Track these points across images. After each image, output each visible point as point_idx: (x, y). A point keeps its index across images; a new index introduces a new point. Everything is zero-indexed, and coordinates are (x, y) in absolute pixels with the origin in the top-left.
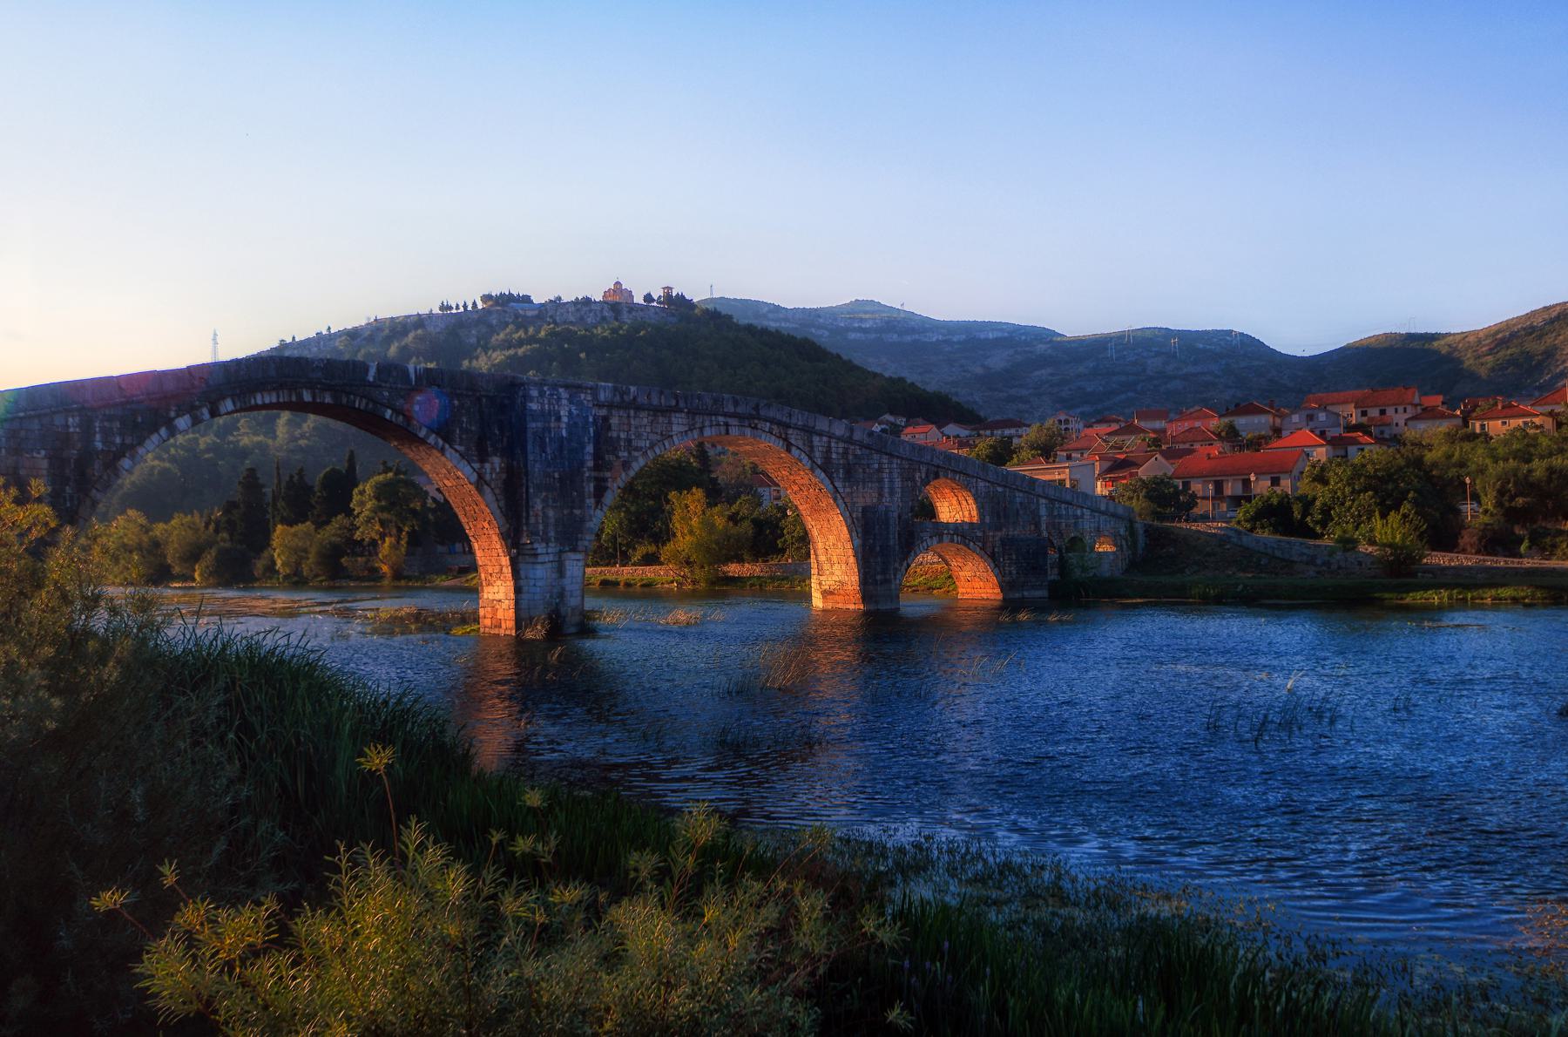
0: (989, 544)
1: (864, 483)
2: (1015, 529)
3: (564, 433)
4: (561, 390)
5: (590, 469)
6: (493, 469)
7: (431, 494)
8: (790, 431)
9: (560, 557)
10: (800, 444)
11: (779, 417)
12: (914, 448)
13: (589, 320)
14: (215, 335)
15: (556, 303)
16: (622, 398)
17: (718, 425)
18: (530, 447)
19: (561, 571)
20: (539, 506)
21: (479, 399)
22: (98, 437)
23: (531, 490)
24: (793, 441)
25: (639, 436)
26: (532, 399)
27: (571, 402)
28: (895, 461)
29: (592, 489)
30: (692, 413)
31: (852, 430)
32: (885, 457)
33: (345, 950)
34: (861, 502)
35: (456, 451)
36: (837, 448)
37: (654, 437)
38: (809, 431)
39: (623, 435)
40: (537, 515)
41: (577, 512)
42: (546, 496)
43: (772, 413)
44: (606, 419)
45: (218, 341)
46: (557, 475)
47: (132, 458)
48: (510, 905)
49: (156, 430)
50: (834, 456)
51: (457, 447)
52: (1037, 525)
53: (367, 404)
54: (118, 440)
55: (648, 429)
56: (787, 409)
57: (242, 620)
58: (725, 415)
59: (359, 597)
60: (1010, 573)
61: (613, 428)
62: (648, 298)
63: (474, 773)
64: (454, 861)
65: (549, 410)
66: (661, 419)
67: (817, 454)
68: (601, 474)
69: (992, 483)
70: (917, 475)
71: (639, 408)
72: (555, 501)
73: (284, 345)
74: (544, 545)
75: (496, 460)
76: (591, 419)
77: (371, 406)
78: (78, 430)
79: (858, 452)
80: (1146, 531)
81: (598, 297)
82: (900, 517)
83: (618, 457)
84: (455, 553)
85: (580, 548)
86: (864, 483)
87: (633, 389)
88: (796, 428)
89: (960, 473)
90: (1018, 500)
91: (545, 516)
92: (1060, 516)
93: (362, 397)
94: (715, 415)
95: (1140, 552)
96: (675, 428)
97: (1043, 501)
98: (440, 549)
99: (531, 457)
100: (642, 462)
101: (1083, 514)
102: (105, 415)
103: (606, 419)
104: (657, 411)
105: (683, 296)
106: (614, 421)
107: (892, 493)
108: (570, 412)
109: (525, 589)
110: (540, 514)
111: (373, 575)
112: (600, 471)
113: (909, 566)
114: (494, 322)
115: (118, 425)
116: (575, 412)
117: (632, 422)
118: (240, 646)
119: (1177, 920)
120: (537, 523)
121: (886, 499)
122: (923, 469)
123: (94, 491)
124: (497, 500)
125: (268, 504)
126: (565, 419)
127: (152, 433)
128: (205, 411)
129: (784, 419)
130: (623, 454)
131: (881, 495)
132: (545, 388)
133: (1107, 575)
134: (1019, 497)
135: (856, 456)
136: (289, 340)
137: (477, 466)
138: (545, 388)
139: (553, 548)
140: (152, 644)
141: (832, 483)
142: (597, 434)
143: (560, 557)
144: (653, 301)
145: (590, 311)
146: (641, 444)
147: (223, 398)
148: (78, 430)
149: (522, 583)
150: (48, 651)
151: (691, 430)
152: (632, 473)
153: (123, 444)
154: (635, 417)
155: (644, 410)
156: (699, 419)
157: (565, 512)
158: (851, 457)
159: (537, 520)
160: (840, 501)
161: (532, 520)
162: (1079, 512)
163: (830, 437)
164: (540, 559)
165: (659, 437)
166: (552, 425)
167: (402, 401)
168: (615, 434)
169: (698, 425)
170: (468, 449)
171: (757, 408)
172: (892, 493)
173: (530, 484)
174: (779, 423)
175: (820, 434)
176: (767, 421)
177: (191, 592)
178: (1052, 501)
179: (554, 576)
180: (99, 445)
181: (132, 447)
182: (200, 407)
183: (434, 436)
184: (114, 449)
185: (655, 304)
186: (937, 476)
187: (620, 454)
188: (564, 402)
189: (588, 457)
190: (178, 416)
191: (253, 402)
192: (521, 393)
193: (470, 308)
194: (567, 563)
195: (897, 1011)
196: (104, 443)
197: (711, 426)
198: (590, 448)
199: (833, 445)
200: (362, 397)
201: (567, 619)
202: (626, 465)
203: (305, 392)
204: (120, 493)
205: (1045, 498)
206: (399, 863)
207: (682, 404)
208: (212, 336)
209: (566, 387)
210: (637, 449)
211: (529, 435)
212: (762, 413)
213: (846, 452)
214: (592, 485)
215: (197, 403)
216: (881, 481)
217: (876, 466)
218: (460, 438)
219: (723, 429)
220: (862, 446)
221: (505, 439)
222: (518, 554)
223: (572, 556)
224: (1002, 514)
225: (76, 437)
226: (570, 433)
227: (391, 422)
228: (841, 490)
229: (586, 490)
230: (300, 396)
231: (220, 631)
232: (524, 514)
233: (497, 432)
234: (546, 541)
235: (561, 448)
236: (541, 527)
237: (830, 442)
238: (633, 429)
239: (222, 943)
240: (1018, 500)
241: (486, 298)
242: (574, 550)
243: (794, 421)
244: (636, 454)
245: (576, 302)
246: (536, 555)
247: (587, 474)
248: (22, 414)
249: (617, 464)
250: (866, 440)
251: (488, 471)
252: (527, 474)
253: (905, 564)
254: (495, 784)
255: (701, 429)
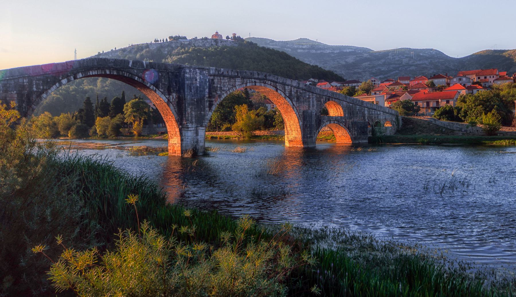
0: (347, 124)
1: (303, 102)
2: (356, 119)
3: (198, 85)
4: (197, 70)
5: (207, 98)
6: (173, 98)
7: (151, 106)
8: (277, 84)
9: (197, 128)
10: (281, 89)
11: (273, 79)
12: (321, 90)
13: (207, 45)
14: (76, 50)
15: (195, 39)
16: (218, 72)
17: (252, 82)
18: (186, 90)
19: (197, 133)
20: (190, 111)
21: (168, 73)
22: (34, 86)
23: (186, 105)
24: (278, 88)
25: (224, 86)
26: (186, 73)
27: (200, 74)
28: (314, 95)
29: (208, 105)
30: (243, 78)
31: (299, 84)
32: (311, 93)
33: (121, 267)
34: (302, 109)
35: (160, 91)
36: (294, 90)
37: (230, 86)
38: (284, 84)
39: (219, 86)
40: (188, 114)
41: (203, 113)
42: (192, 107)
44: (213, 80)
45: (74, 53)
46: (195, 100)
47: (47, 94)
48: (179, 251)
49: (55, 84)
50: (293, 93)
51: (160, 90)
52: (364, 117)
53: (129, 75)
54: (41, 87)
55: (228, 84)
56: (276, 77)
57: (85, 150)
58: (255, 79)
59: (126, 142)
60: (355, 134)
61: (215, 83)
62: (228, 37)
63: (166, 204)
64: (159, 235)
65: (193, 77)
66: (232, 80)
67: (287, 92)
68: (211, 99)
69: (348, 103)
70: (322, 100)
71: (224, 76)
72: (195, 109)
73: (99, 54)
74: (191, 124)
75: (174, 95)
76: (207, 80)
77: (130, 75)
78: (27, 84)
80: (402, 119)
81: (210, 37)
82: (316, 114)
83: (217, 93)
84: (160, 127)
85: (204, 125)
86: (303, 102)
87: (222, 69)
89: (337, 99)
90: (357, 108)
91: (191, 114)
92: (372, 114)
93: (127, 72)
94: (251, 78)
95: (400, 126)
96: (237, 83)
97: (366, 109)
98: (155, 126)
99: (186, 93)
100: (225, 95)
101: (380, 114)
102: (37, 78)
103: (213, 80)
104: (231, 77)
105: (240, 37)
106: (216, 81)
107: (313, 106)
108: (200, 78)
109: (184, 140)
110: (190, 113)
111: (131, 135)
112: (210, 98)
113: (319, 131)
114: (174, 46)
115: (41, 82)
116: (202, 78)
117: (222, 81)
118: (84, 160)
119: (413, 256)
120: (189, 116)
121: (311, 108)
122: (324, 97)
123: (33, 105)
124: (175, 108)
125: (94, 110)
126: (198, 80)
127: (53, 85)
128: (72, 77)
129: (275, 80)
130: (219, 92)
131: (309, 107)
132: (191, 69)
133: (389, 135)
134: (358, 107)
135: (300, 93)
136: (101, 52)
137: (167, 96)
138: (191, 69)
139: (194, 125)
140: (53, 159)
141: (292, 102)
142: (210, 85)
143: (197, 128)
144: (229, 38)
145: (207, 42)
146: (225, 89)
147: (79, 73)
148: (27, 84)
149: (183, 137)
150: (17, 162)
151: (243, 84)
152: (222, 99)
153: (43, 89)
154: (223, 79)
155: (226, 77)
156: (245, 80)
157: (199, 113)
158: (299, 94)
159: (188, 115)
160: (295, 109)
161: (187, 115)
162: (379, 113)
163: (291, 86)
164: (190, 129)
165: (231, 87)
166: (194, 82)
167: (141, 74)
168: (216, 85)
169: (245, 82)
170: (164, 91)
171: (266, 76)
172: (313, 106)
173: (186, 103)
174: (274, 82)
175: (288, 85)
176: (269, 80)
177: (67, 141)
178: (369, 109)
179: (195, 135)
180: (35, 89)
181: (46, 90)
182: (71, 76)
183: (152, 86)
184: (40, 90)
185: (230, 40)
186: (329, 100)
187: (218, 92)
188: (198, 74)
189: (206, 93)
190: (62, 79)
191: (89, 74)
192: (183, 71)
193: (165, 41)
194: (199, 130)
195: (315, 288)
196: (36, 88)
197: (250, 82)
198: (207, 90)
199: (292, 89)
200: (127, 72)
201: (199, 150)
202: (220, 96)
203: (107, 71)
204: (42, 106)
205: (367, 108)
206: (140, 236)
207: (239, 75)
208: (74, 51)
209: (199, 69)
210: (224, 91)
211: (186, 86)
212: (268, 78)
213: (297, 92)
214: (208, 103)
215: (69, 74)
216: (309, 102)
217: (308, 96)
218: (162, 87)
219: (254, 84)
220: (303, 89)
221: (177, 87)
222: (182, 127)
223: (201, 128)
224: (352, 113)
225: (27, 87)
226: (200, 85)
227: (137, 81)
228: (295, 105)
229: (206, 105)
230: (105, 72)
231: (77, 154)
232: (184, 114)
233: (174, 84)
234: (192, 123)
235: (197, 90)
236: (190, 118)
237: (291, 88)
238: (222, 84)
239: (78, 264)
240: (357, 108)
241: (171, 38)
242: (202, 126)
243: (279, 81)
244: (223, 92)
245: (202, 39)
246: (188, 128)
247: (206, 99)
248: (8, 78)
249: (217, 96)
250: (304, 88)
251: (171, 98)
252: (185, 99)
253: (318, 131)
254: (174, 208)
255: (246, 83)
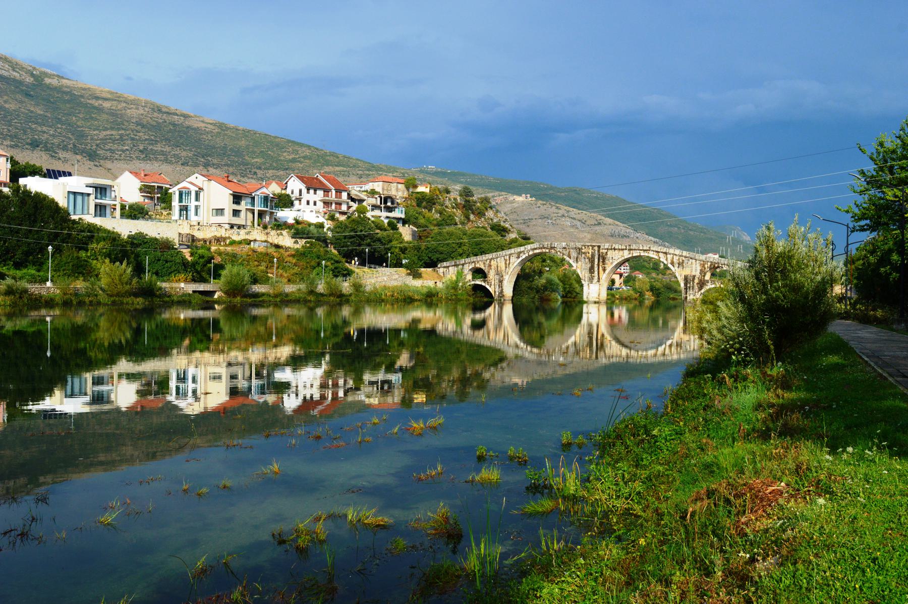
30: (630, 250)
43: (654, 249)
44: (606, 253)
50: (675, 260)
70: (706, 266)
71: (615, 249)
79: (684, 259)
88: (662, 252)
103: (606, 253)
106: (608, 253)
122: (709, 264)
126: (590, 253)
130: (611, 261)
139: (587, 283)
175: (670, 254)
202: (612, 263)
207: (628, 248)
213: (679, 259)
216: (692, 267)
220: (686, 257)
242: (592, 283)
